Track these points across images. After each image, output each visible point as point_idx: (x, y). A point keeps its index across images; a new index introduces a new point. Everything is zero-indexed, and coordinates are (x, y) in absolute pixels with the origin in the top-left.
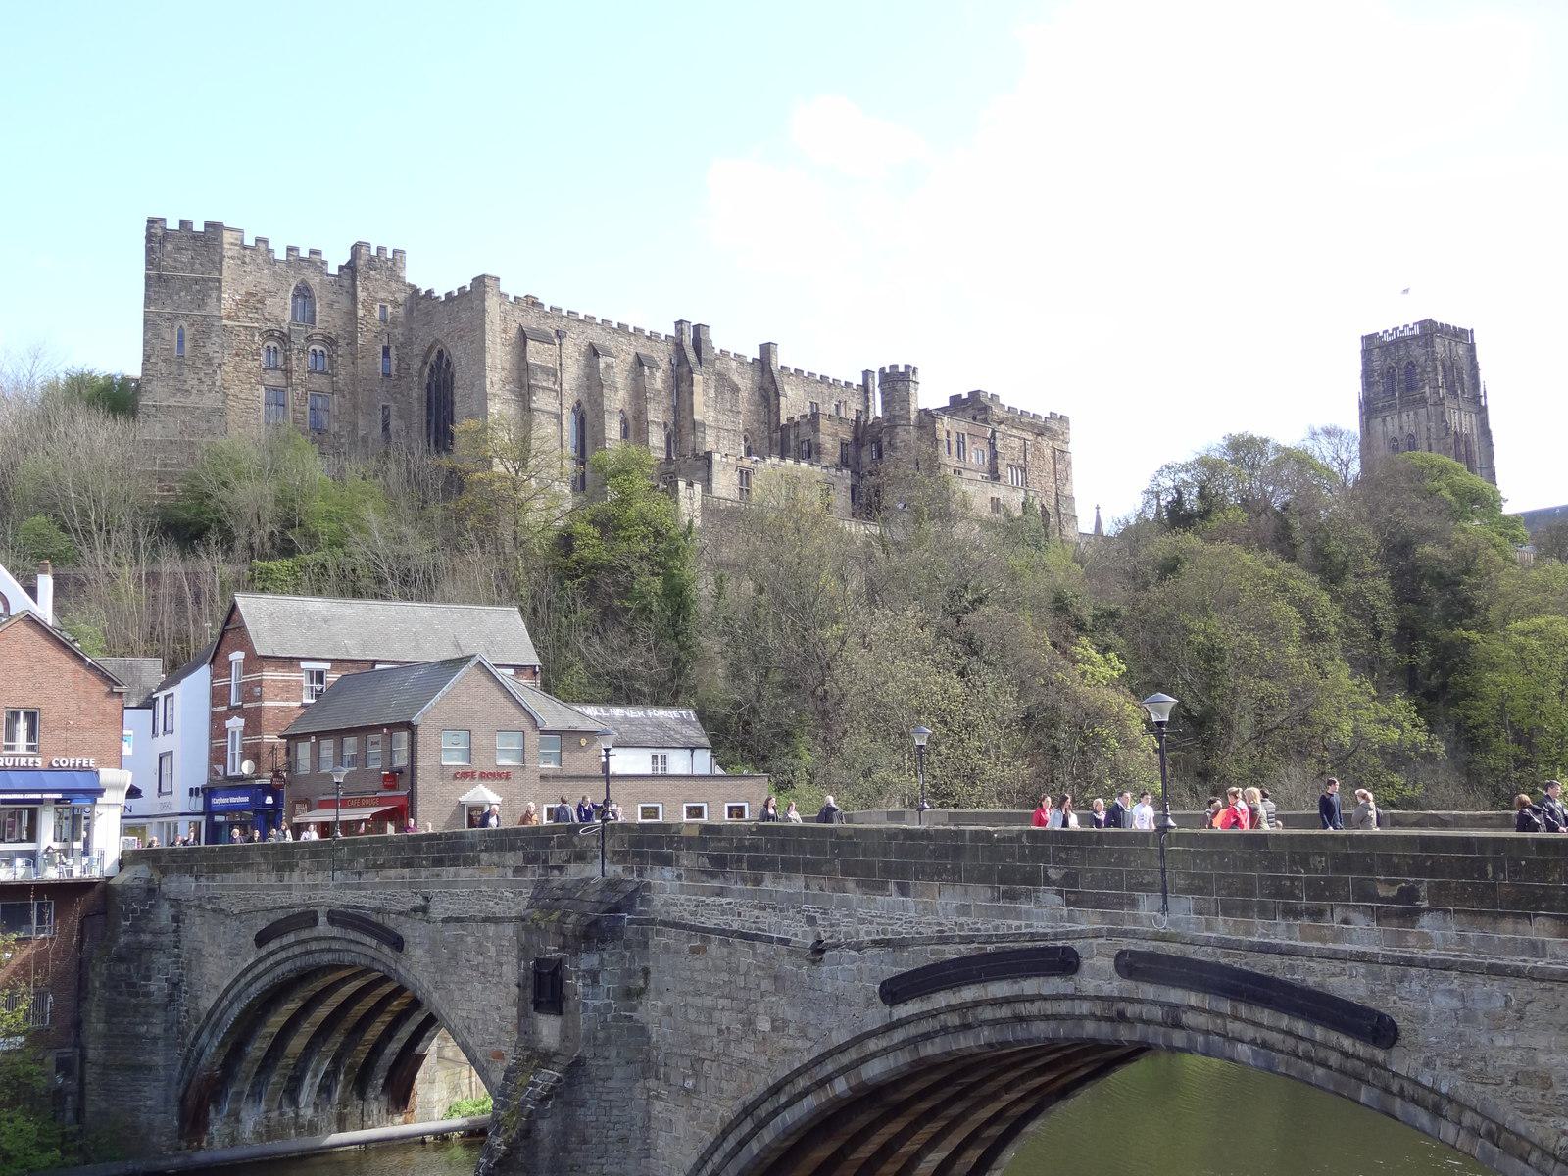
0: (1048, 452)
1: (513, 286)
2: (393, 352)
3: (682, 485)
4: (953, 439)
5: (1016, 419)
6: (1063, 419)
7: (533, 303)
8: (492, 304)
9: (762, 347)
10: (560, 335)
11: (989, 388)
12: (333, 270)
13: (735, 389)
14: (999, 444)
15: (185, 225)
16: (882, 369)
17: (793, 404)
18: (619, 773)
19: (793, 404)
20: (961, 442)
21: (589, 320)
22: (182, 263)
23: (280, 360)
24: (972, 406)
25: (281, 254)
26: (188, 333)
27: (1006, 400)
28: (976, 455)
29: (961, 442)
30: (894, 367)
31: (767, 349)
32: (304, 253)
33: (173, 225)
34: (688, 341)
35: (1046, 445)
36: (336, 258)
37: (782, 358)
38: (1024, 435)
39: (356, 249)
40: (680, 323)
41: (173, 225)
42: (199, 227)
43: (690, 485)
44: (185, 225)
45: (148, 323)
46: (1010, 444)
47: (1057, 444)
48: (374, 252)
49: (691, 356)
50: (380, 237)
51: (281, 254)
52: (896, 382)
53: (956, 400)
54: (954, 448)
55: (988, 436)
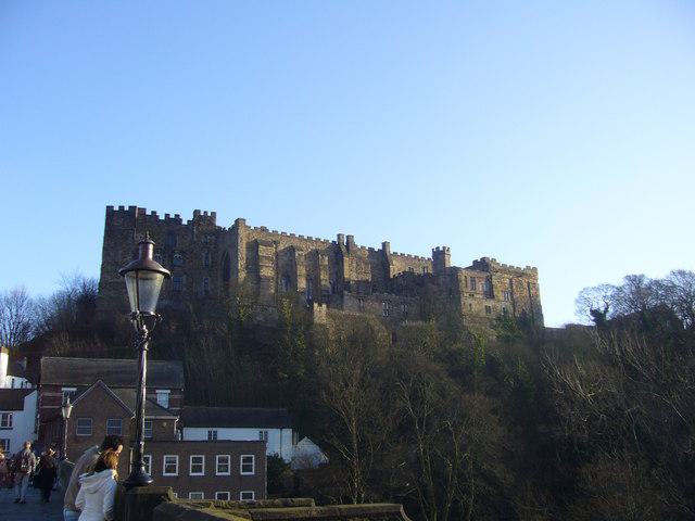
0: (525, 285)
1: (253, 223)
2: (210, 256)
3: (316, 305)
5: (506, 270)
6: (535, 269)
7: (264, 229)
8: (241, 231)
9: (338, 235)
12: (185, 222)
15: (121, 208)
17: (396, 268)
18: (191, 439)
19: (396, 268)
20: (473, 280)
22: (125, 228)
24: (482, 265)
25: (162, 217)
27: (501, 260)
28: (481, 286)
29: (473, 280)
30: (438, 248)
31: (385, 245)
32: (172, 216)
33: (116, 208)
35: (524, 280)
36: (187, 217)
37: (392, 249)
39: (196, 212)
40: (338, 235)
41: (116, 208)
42: (127, 209)
43: (320, 305)
44: (121, 208)
45: (104, 249)
46: (501, 283)
47: (531, 280)
50: (206, 208)
51: (162, 217)
52: (440, 255)
53: (475, 262)
54: (469, 285)
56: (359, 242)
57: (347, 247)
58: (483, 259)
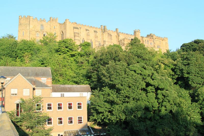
4: (146, 41)
5: (158, 38)
10: (80, 28)
11: (153, 33)
13: (111, 35)
14: (155, 42)
16: (134, 31)
21: (85, 26)
23: (39, 35)
24: (150, 36)
25: (39, 20)
26: (24, 32)
32: (42, 19)
34: (103, 28)
35: (164, 42)
38: (160, 40)
48: (53, 18)
49: (103, 31)
55: (153, 40)
56: (108, 28)
57: (104, 29)
58: (150, 34)
